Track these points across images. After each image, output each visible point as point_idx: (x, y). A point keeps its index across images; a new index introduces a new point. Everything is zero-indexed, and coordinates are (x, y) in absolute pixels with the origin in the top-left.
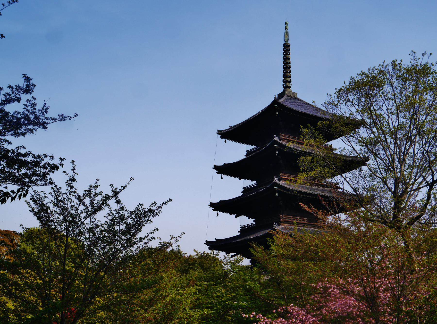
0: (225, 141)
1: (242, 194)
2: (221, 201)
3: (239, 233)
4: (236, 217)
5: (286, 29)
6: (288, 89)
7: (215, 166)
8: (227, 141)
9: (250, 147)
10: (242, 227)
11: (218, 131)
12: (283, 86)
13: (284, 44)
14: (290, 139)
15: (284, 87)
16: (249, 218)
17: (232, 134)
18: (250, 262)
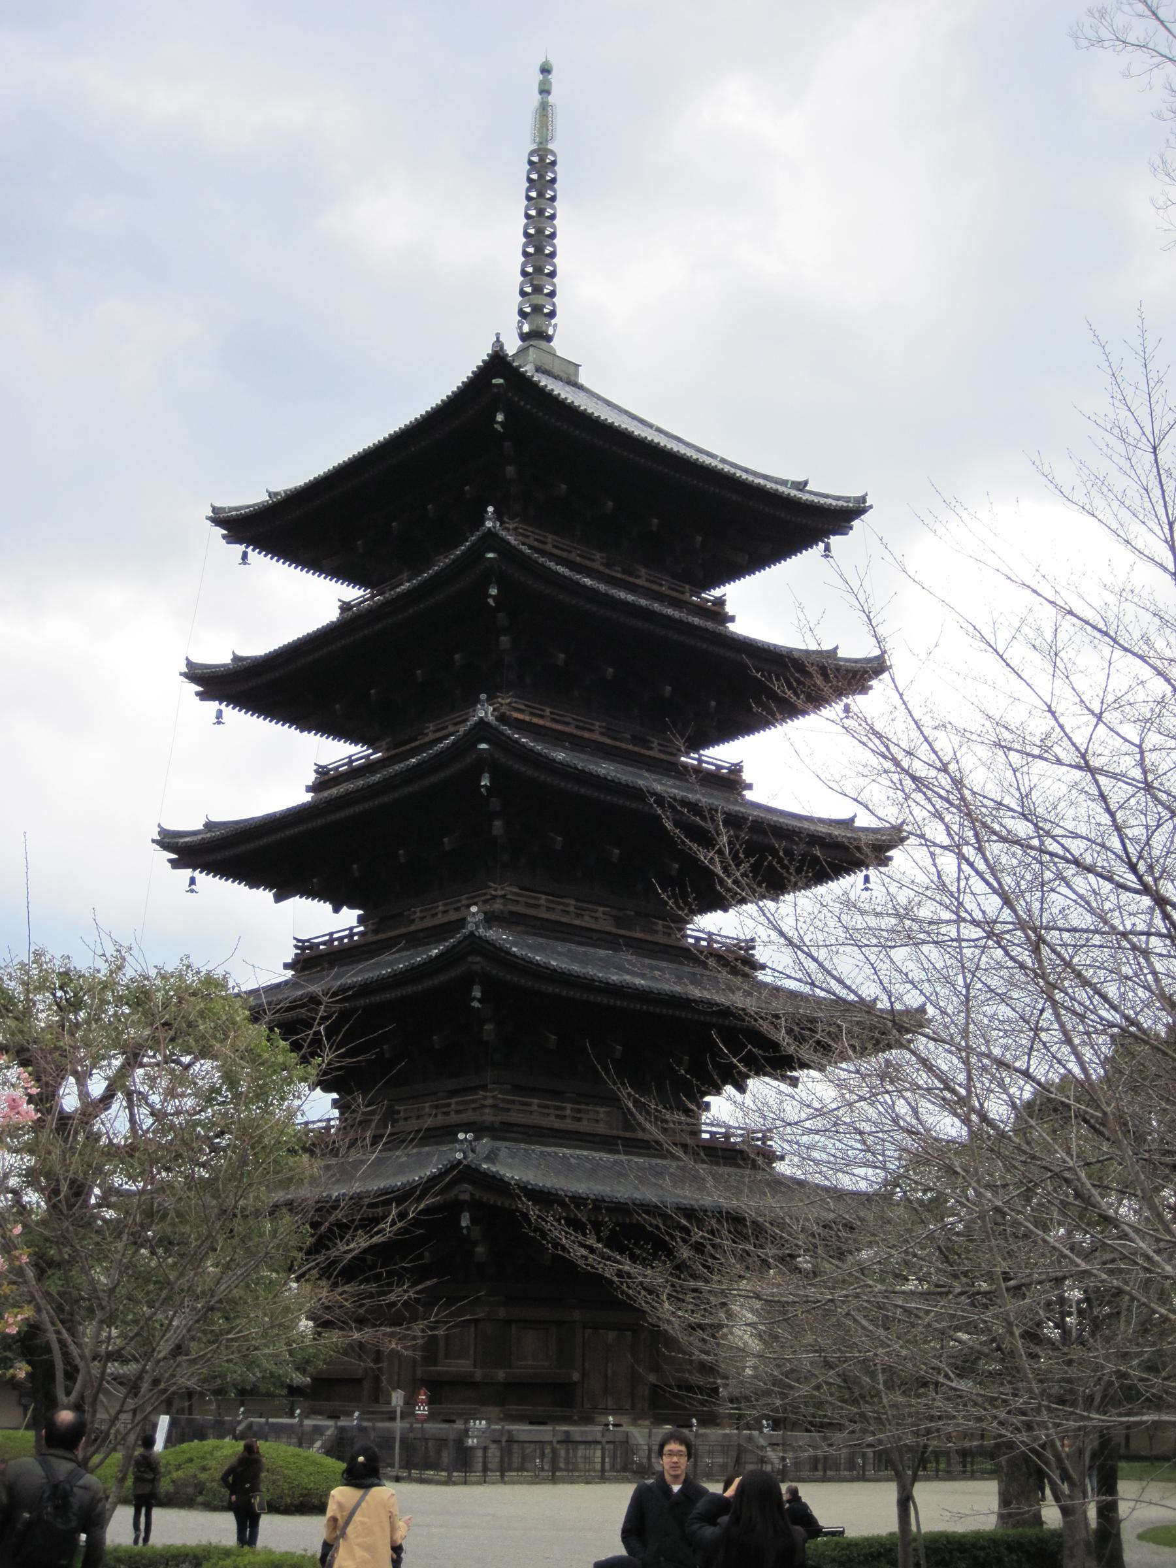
0: (245, 556)
1: (308, 797)
2: (209, 826)
3: (290, 974)
4: (279, 898)
5: (545, 91)
6: (543, 344)
7: (190, 664)
8: (254, 556)
9: (353, 593)
10: (304, 946)
11: (215, 509)
12: (520, 328)
13: (532, 153)
14: (549, 547)
15: (524, 337)
16: (336, 910)
17: (278, 528)
18: (335, 1104)
